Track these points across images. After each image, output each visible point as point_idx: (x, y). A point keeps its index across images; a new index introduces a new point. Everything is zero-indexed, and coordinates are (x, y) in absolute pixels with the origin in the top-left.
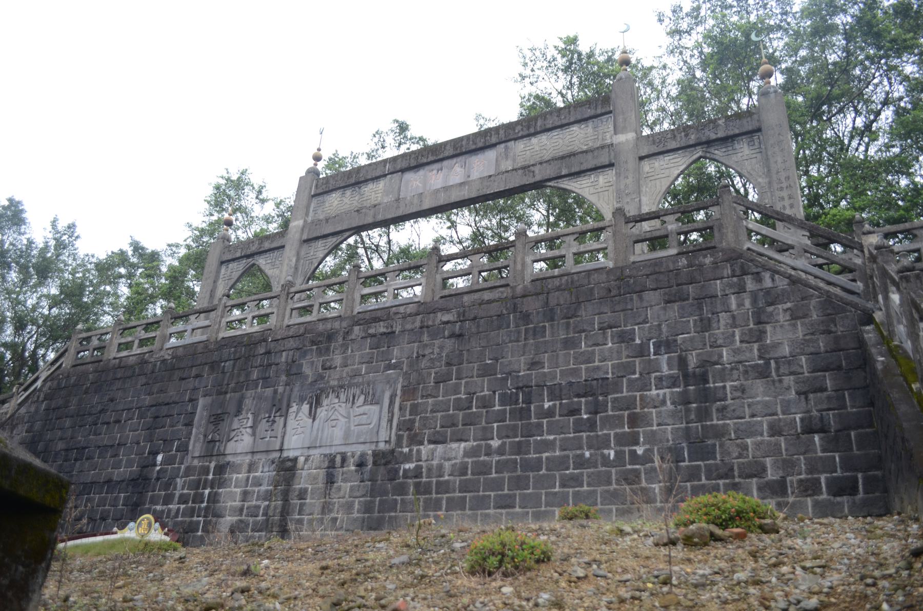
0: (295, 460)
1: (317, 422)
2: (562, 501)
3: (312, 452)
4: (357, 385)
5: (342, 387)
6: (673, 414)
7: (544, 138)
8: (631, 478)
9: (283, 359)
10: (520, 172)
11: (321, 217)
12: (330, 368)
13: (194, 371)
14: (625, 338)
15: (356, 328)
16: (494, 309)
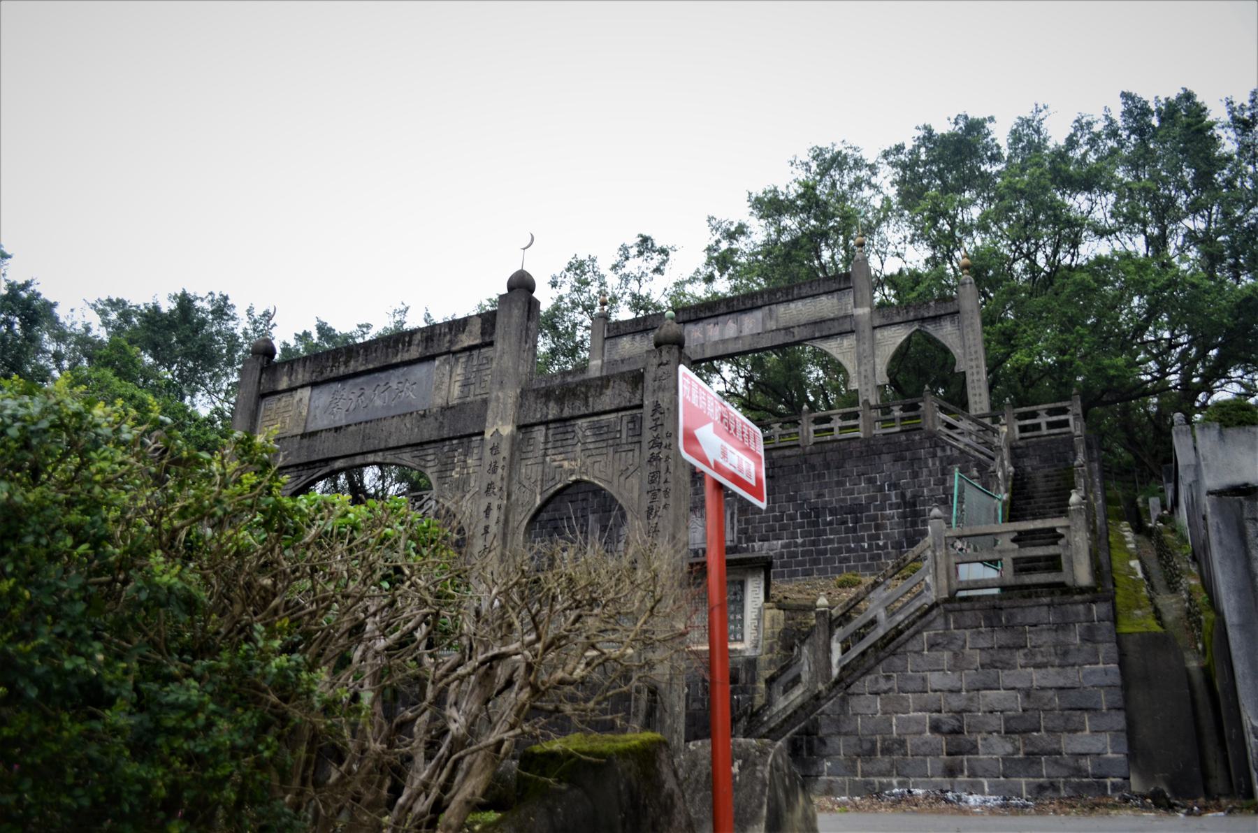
6: (898, 524)
7: (800, 304)
11: (617, 357)
13: (580, 497)
14: (871, 481)
16: (793, 461)
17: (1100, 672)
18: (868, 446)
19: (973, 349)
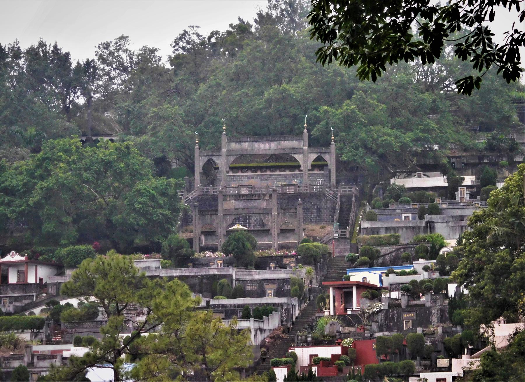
8: (311, 220)
14: (311, 203)
17: (349, 247)
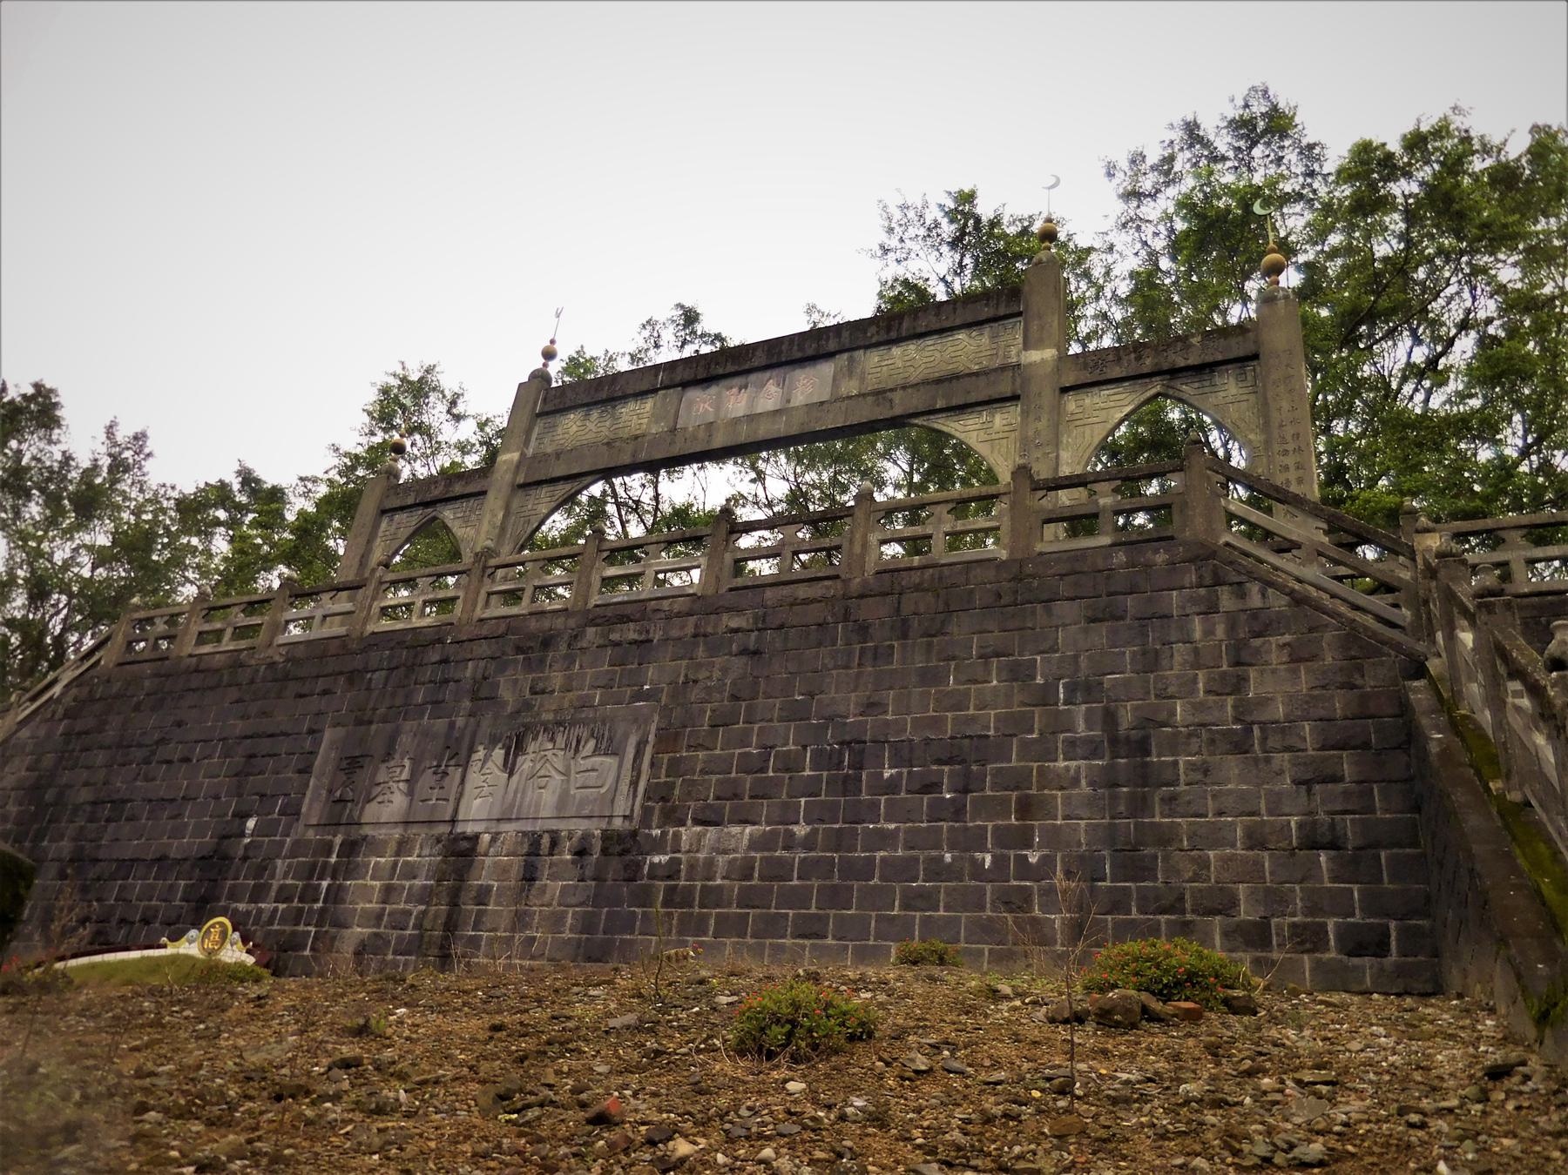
0: (476, 838)
1: (515, 778)
2: (901, 931)
3: (505, 827)
4: (584, 722)
5: (559, 724)
6: (1091, 802)
7: (911, 348)
8: (1016, 902)
9: (468, 673)
10: (870, 399)
11: (549, 450)
12: (543, 692)
13: (321, 685)
14: (1019, 674)
15: (591, 631)
16: (815, 613)
18: (1017, 579)
19: (1289, 431)
